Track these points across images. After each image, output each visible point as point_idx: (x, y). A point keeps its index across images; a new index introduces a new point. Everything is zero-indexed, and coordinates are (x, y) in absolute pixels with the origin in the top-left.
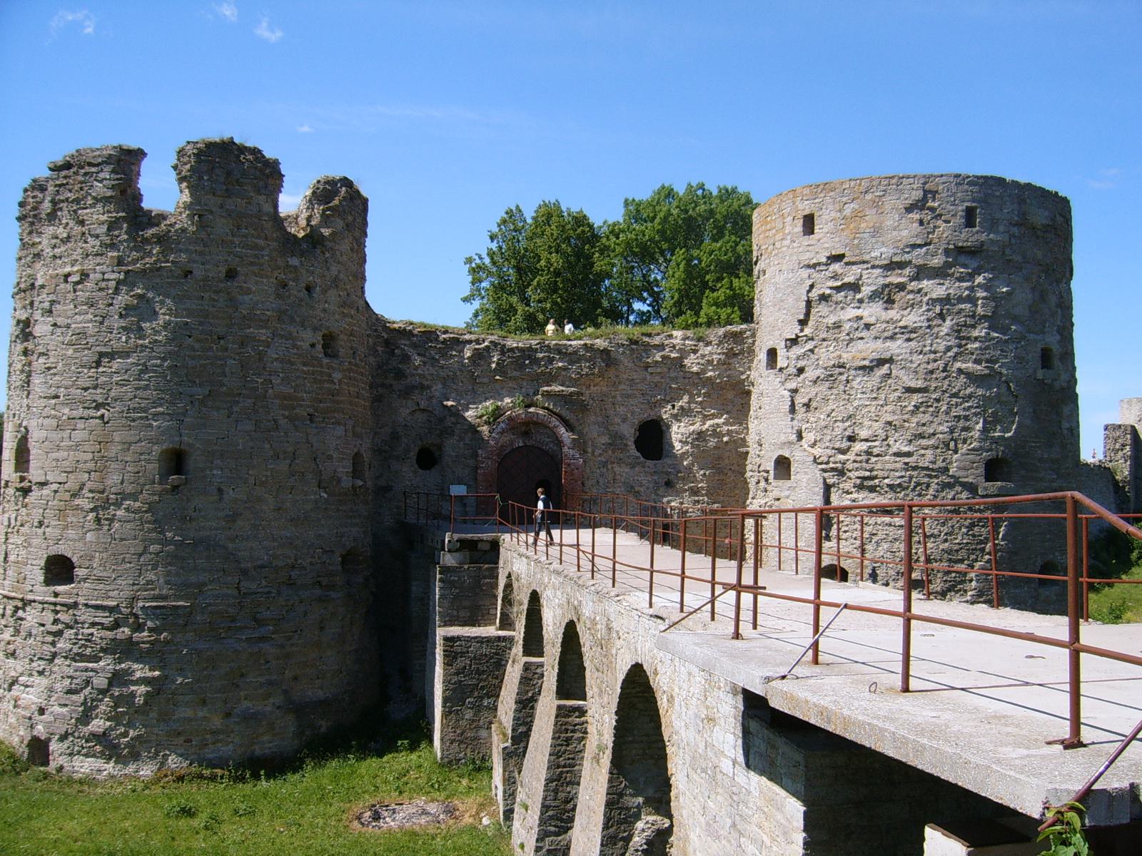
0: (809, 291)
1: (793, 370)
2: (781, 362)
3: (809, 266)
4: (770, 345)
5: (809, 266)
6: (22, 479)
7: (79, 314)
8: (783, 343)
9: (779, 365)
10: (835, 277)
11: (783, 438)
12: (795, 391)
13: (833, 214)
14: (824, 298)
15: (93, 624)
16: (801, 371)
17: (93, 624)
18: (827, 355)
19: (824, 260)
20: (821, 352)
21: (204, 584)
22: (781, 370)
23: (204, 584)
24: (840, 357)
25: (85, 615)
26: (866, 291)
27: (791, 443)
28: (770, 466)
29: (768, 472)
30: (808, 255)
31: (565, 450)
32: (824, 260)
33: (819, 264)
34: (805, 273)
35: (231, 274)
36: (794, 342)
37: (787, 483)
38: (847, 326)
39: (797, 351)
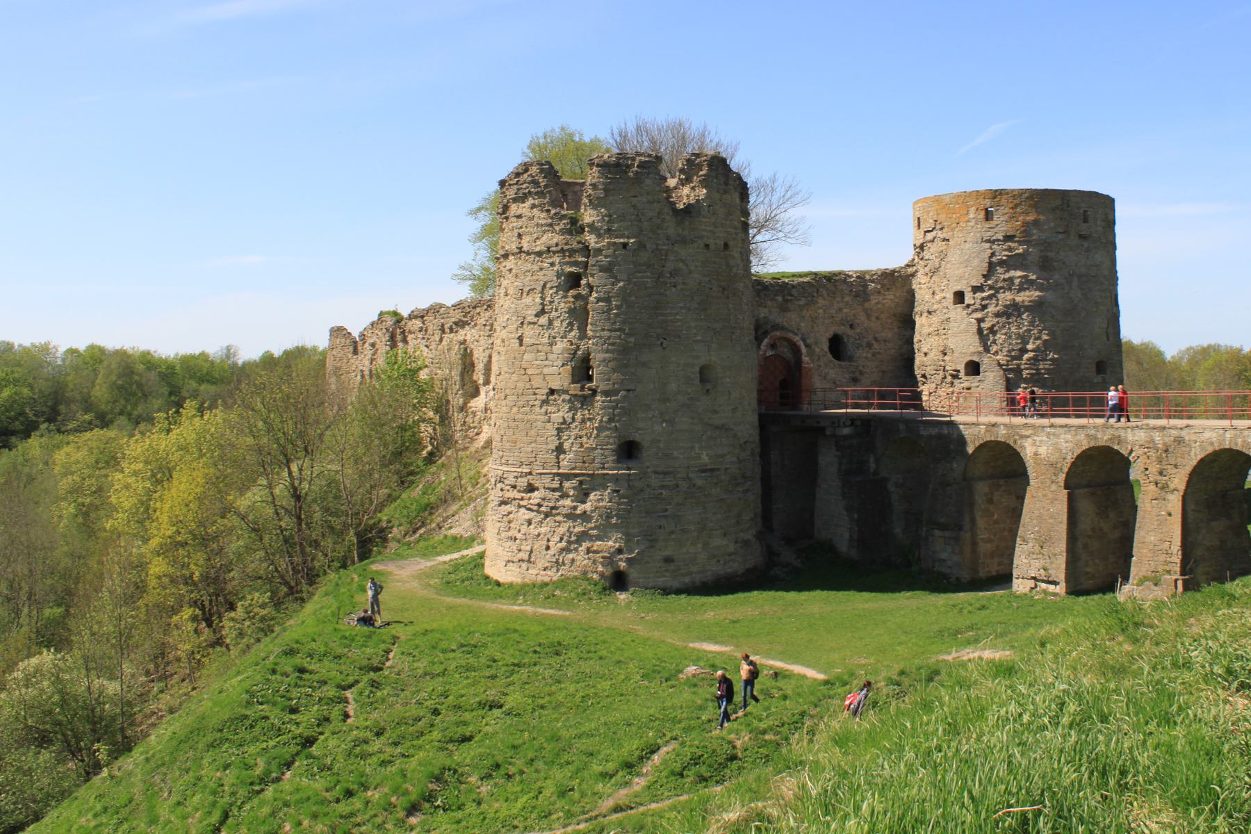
0: (991, 257)
1: (978, 306)
2: (968, 300)
3: (988, 241)
4: (958, 288)
5: (988, 241)
6: (582, 388)
7: (639, 272)
8: (970, 289)
9: (967, 302)
10: (1010, 249)
11: (972, 349)
12: (980, 321)
13: (1007, 210)
14: (1001, 263)
15: (663, 487)
16: (984, 307)
17: (663, 487)
18: (1006, 297)
19: (1001, 238)
20: (1001, 296)
21: (725, 455)
22: (968, 306)
23: (725, 455)
24: (1014, 300)
25: (655, 481)
26: (1030, 258)
27: (979, 352)
28: (961, 367)
29: (958, 371)
30: (989, 234)
31: (803, 358)
32: (1001, 238)
33: (998, 240)
34: (988, 245)
35: (726, 246)
36: (976, 289)
37: (978, 378)
38: (1017, 281)
39: (979, 295)
